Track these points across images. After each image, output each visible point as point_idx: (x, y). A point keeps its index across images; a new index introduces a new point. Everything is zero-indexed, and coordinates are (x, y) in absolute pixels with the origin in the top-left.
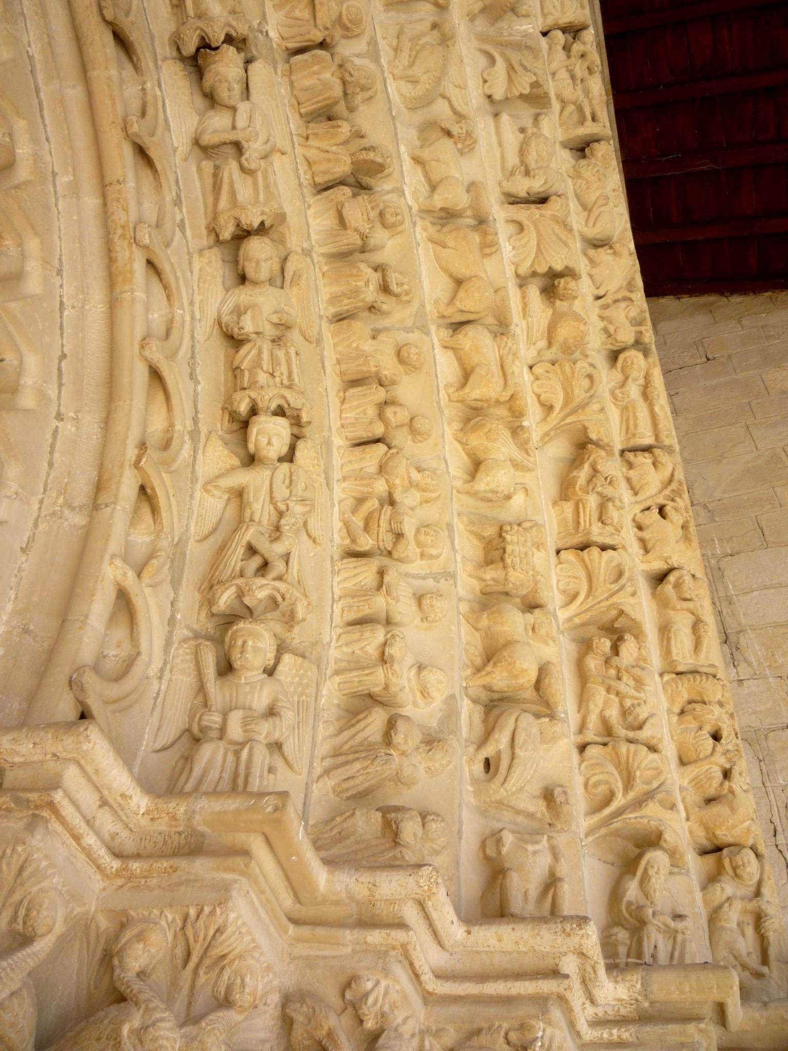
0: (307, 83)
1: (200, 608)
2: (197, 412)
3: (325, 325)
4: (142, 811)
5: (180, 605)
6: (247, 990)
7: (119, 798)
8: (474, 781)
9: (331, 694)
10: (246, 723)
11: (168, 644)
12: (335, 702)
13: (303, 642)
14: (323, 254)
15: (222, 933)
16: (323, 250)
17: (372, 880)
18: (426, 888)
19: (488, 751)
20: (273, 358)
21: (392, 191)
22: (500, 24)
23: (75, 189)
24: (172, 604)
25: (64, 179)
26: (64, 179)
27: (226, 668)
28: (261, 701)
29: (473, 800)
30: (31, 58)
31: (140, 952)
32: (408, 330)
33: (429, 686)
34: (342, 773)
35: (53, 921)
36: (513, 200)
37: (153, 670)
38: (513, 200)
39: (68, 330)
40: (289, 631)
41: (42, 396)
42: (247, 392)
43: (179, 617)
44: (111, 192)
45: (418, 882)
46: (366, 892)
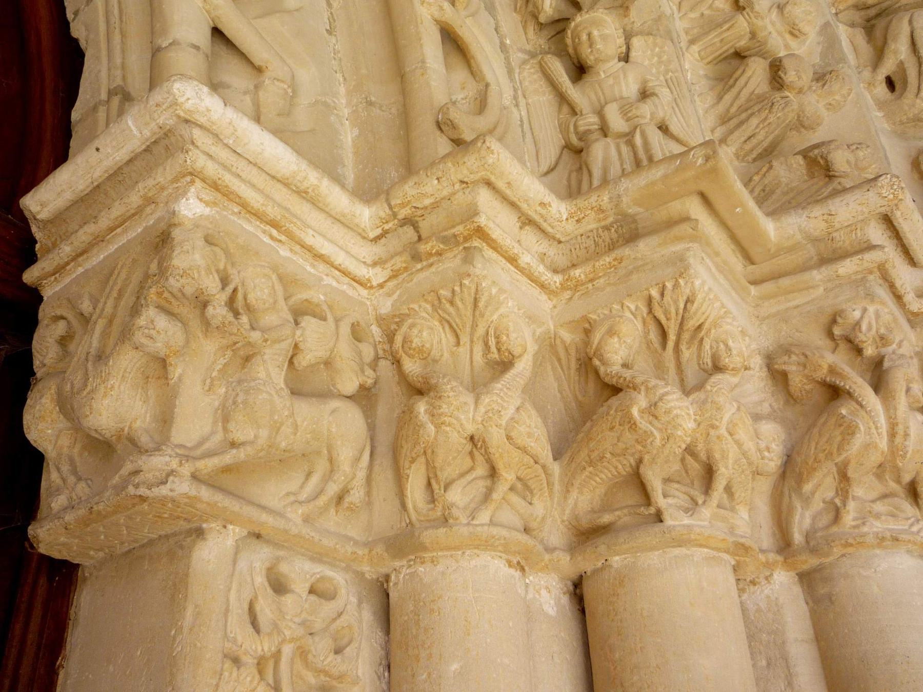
1: (525, 28)
4: (564, 217)
5: (504, 29)
6: (734, 352)
7: (539, 208)
8: (881, 105)
9: (693, 66)
10: (625, 112)
11: (510, 72)
12: (702, 72)
13: (645, 22)
15: (693, 302)
17: (825, 211)
18: (891, 196)
19: (888, 67)
24: (496, 30)
27: (580, 70)
28: (630, 88)
29: (886, 126)
31: (617, 345)
33: (797, 22)
34: (739, 136)
35: (524, 340)
37: (507, 100)
40: (625, 16)
43: (508, 42)
45: (880, 194)
46: (823, 225)
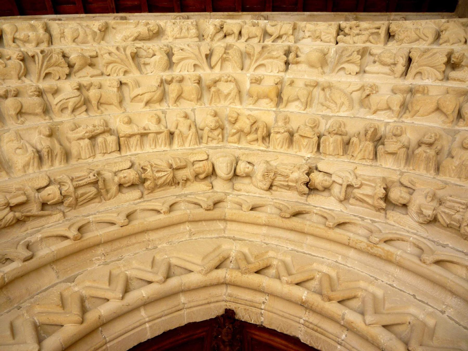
0: (331, 148)
2: (463, 252)
3: (438, 178)
14: (404, 167)
16: (402, 165)
20: (450, 208)
21: (385, 127)
22: (329, 61)
23: (345, 257)
25: (340, 259)
26: (340, 259)
30: (292, 250)
32: (454, 140)
36: (406, 73)
38: (406, 73)
39: (403, 288)
41: (431, 314)
42: (462, 226)
44: (352, 244)
